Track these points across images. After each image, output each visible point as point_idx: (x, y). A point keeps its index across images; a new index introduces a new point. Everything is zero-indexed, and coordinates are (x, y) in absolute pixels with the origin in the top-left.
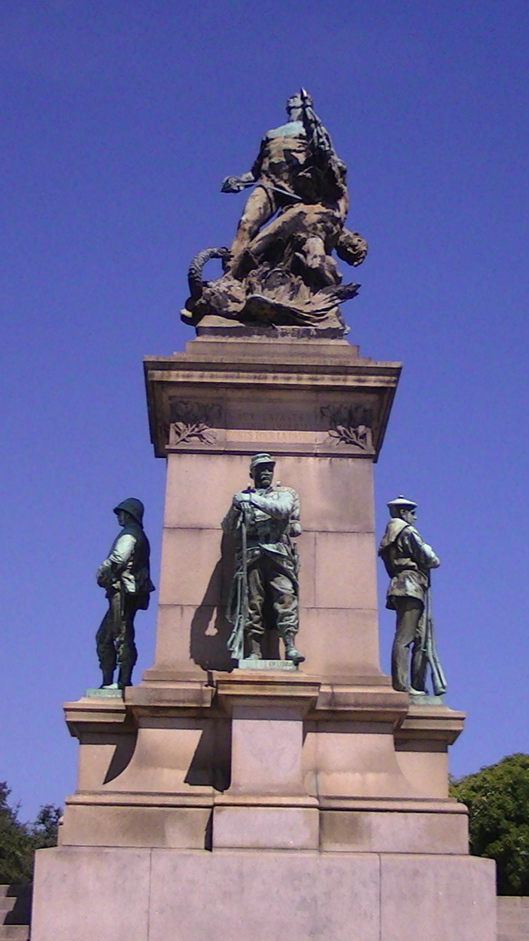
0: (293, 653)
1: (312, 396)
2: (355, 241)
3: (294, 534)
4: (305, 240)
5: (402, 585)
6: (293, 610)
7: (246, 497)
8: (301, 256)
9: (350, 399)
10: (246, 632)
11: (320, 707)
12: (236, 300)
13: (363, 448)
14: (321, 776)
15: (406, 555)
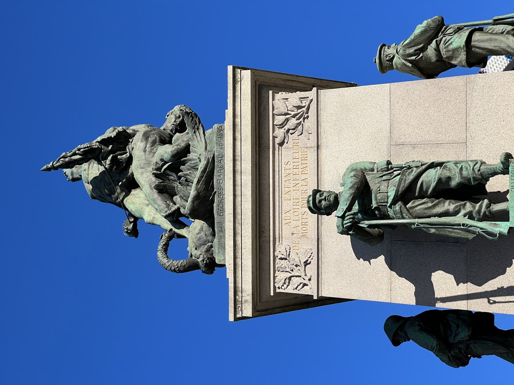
6: (457, 167)
13: (312, 100)
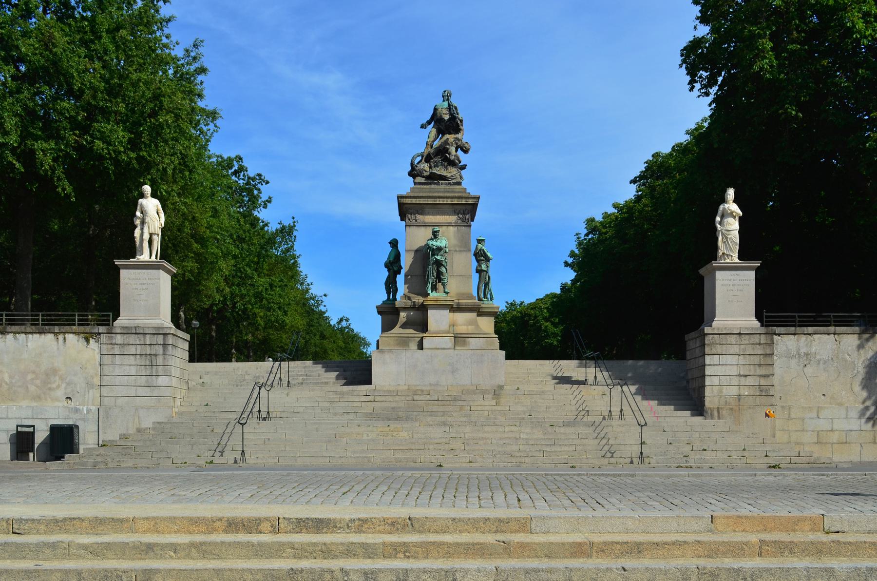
0: (446, 291)
1: (451, 206)
2: (466, 145)
3: (446, 252)
4: (449, 149)
5: (480, 266)
7: (430, 242)
8: (447, 155)
9: (464, 207)
10: (432, 284)
11: (454, 306)
12: (426, 171)
14: (455, 327)
15: (482, 256)
